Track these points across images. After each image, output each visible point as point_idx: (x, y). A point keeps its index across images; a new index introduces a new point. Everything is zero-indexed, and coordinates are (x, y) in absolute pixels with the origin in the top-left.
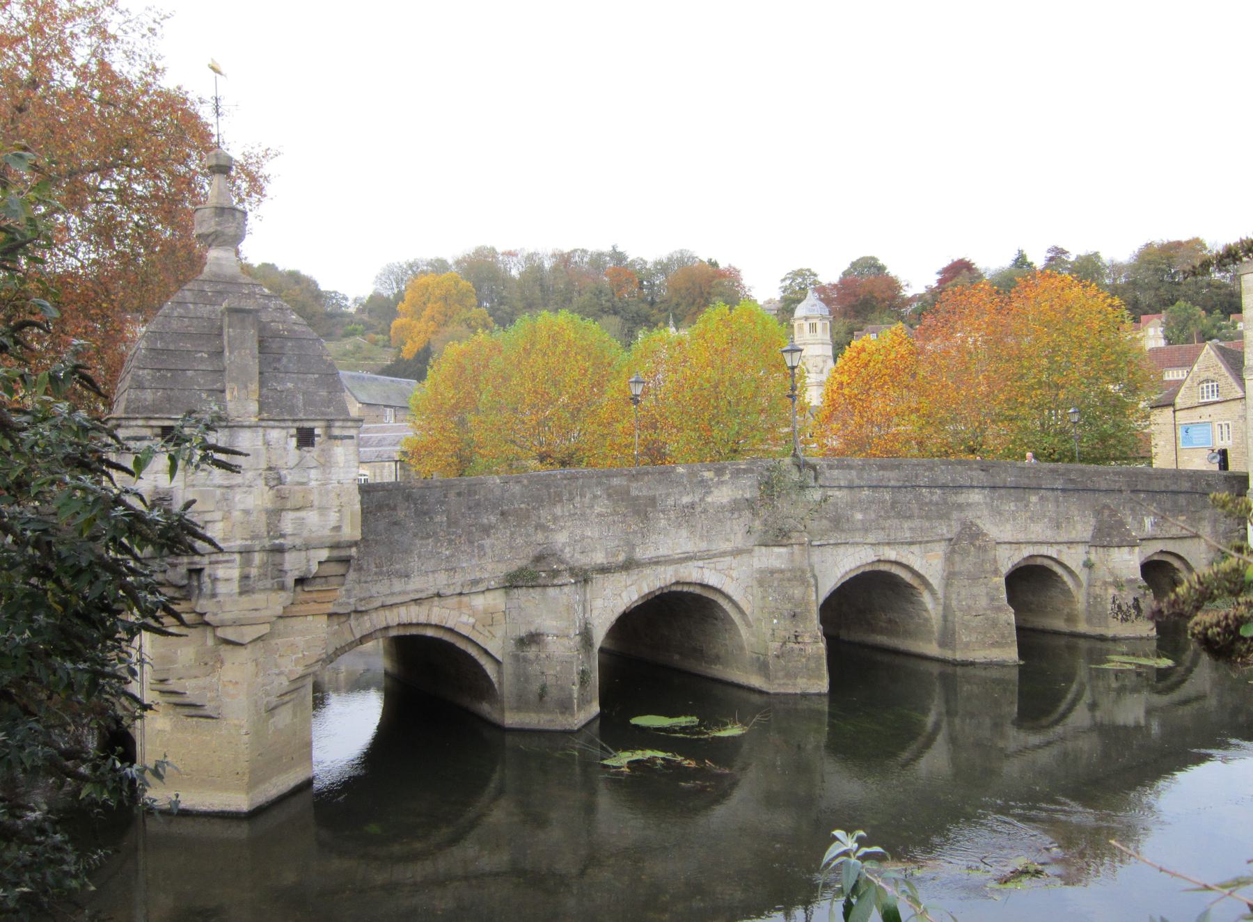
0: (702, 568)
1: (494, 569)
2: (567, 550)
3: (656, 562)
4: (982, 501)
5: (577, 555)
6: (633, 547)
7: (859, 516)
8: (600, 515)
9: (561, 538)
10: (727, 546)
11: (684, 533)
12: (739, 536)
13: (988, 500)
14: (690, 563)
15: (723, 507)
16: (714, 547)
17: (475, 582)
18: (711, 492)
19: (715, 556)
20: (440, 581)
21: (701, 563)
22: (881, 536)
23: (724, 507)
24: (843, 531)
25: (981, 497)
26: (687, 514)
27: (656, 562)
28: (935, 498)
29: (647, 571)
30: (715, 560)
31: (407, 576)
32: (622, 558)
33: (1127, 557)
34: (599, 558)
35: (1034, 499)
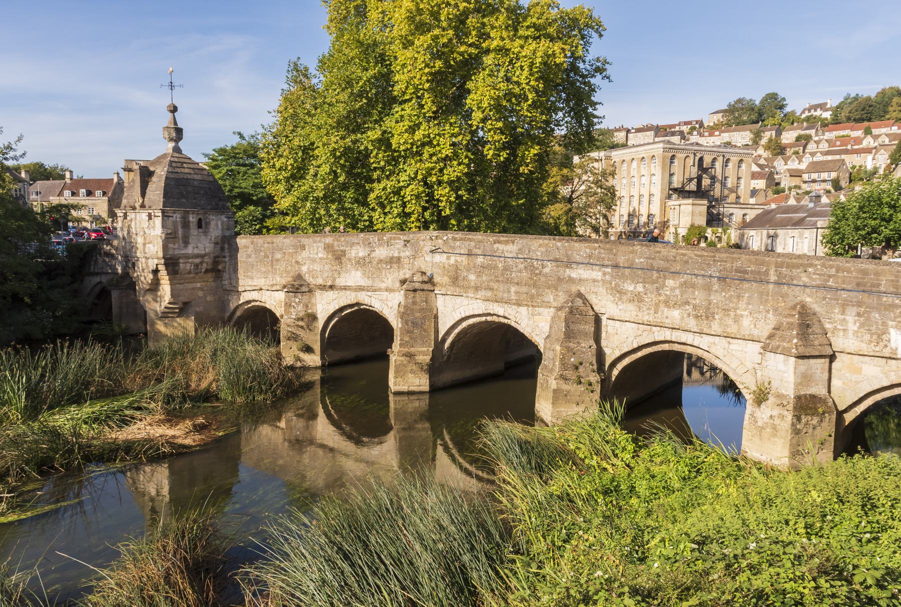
0: (370, 297)
1: (281, 280)
2: (307, 275)
3: (345, 288)
4: (599, 278)
5: (311, 279)
6: (334, 279)
7: (472, 277)
8: (321, 259)
9: (304, 269)
10: (383, 286)
11: (359, 274)
12: (390, 280)
13: (608, 277)
14: (363, 292)
15: (381, 261)
16: (375, 285)
17: (272, 285)
18: (375, 251)
19: (375, 291)
20: (261, 282)
21: (369, 294)
22: (489, 294)
23: (381, 261)
24: (459, 287)
25: (600, 274)
26: (361, 263)
27: (345, 288)
28: (547, 270)
29: (343, 293)
30: (377, 293)
31: (252, 278)
32: (329, 283)
33: (781, 366)
34: (320, 281)
35: (670, 283)
